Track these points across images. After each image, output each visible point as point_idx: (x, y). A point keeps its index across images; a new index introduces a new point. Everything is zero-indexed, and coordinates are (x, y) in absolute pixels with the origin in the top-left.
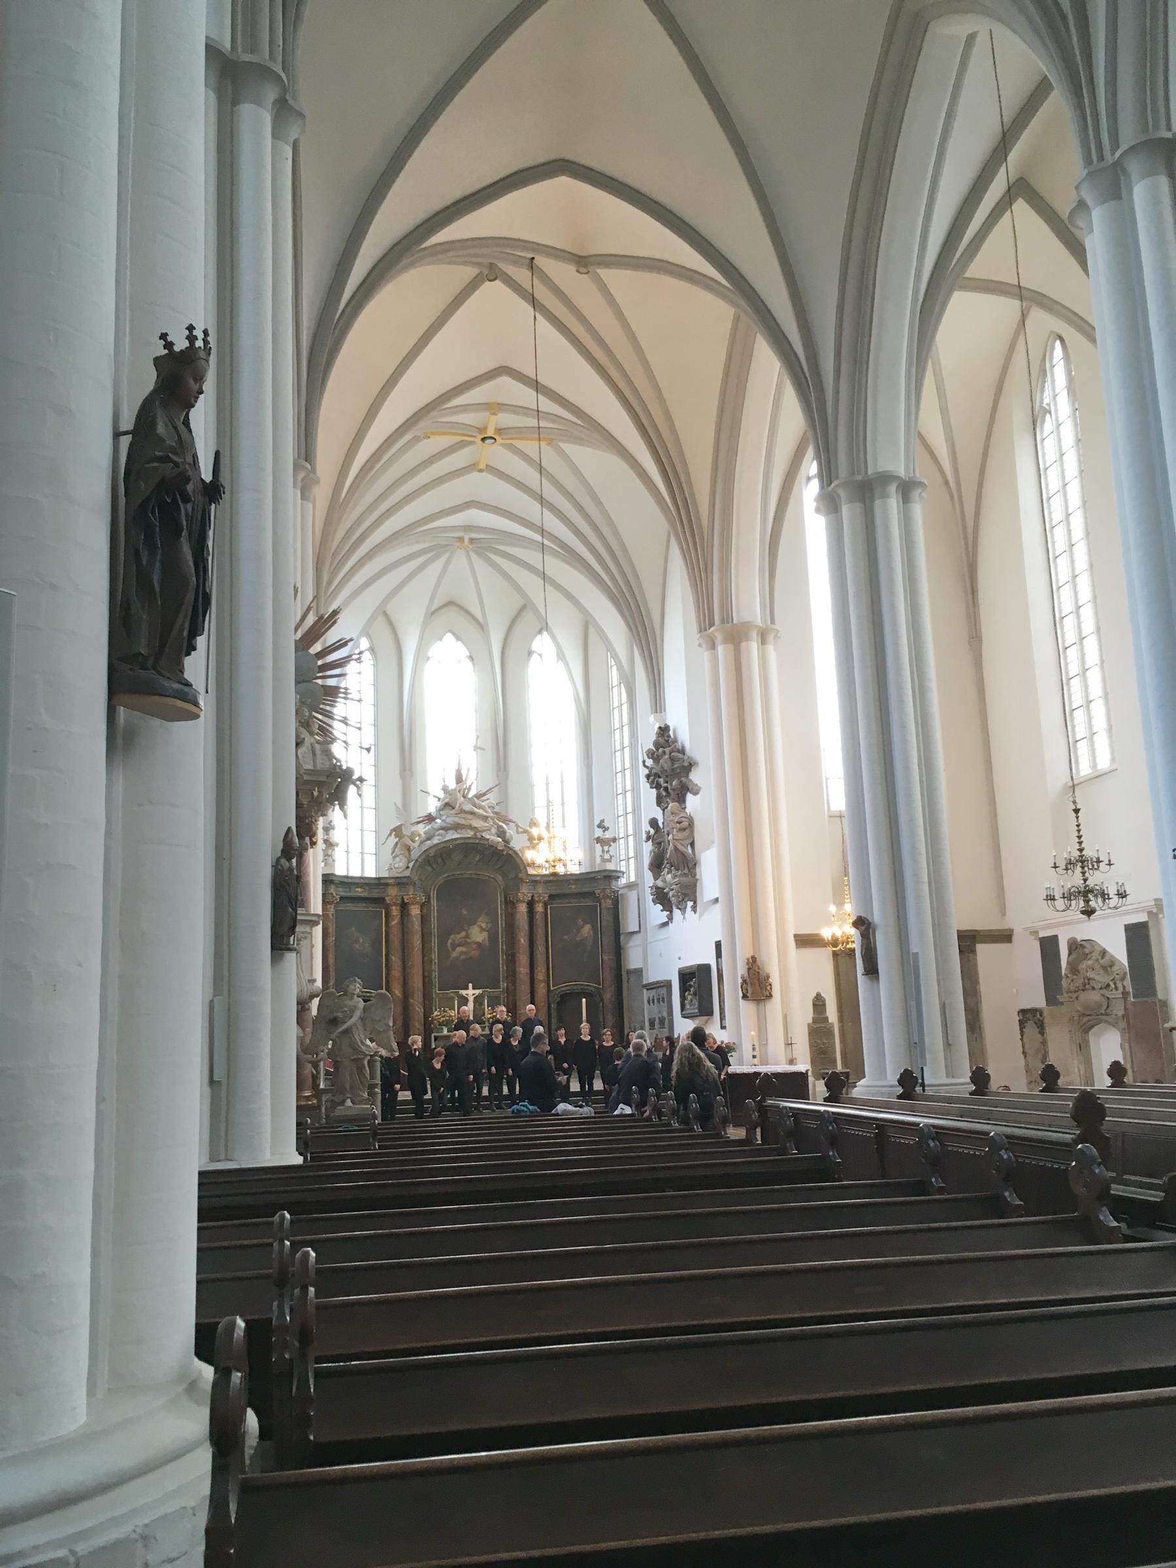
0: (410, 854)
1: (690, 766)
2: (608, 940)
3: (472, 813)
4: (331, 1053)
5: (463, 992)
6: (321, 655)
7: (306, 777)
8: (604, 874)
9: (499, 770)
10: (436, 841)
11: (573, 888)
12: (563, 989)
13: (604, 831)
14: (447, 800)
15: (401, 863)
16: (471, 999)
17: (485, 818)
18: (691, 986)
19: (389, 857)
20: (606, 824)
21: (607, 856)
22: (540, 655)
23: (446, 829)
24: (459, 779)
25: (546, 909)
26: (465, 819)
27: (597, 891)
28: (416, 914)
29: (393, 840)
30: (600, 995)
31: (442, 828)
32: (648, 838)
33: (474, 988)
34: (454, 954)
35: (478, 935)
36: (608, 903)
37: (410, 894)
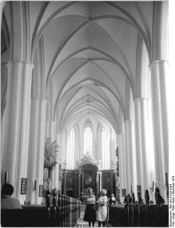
2: (112, 182)
6: (54, 146)
7: (50, 163)
15: (77, 167)
19: (75, 167)
24: (87, 153)
29: (76, 163)
30: (111, 191)
31: (84, 161)
34: (86, 183)
35: (90, 180)
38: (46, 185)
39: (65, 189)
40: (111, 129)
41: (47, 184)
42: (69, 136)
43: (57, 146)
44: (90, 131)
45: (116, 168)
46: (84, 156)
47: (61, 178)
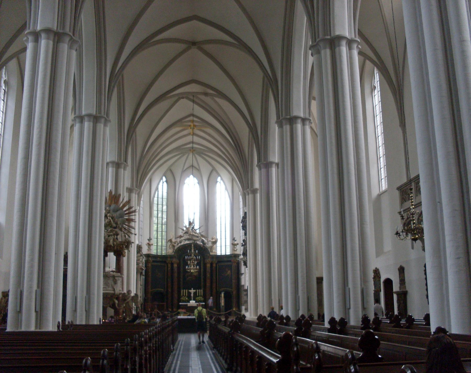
0: (174, 248)
3: (193, 235)
4: (124, 307)
5: (190, 291)
6: (125, 211)
7: (118, 243)
9: (206, 220)
10: (182, 244)
11: (225, 259)
14: (186, 231)
17: (198, 237)
20: (235, 239)
21: (235, 249)
22: (220, 183)
23: (185, 240)
24: (190, 224)
27: (232, 260)
28: (176, 267)
29: (169, 243)
30: (232, 292)
32: (242, 246)
33: (193, 289)
37: (175, 260)
38: (112, 285)
39: (150, 290)
40: (233, 180)
41: (113, 283)
42: (157, 192)
43: (133, 209)
44: (194, 184)
45: (242, 253)
46: (185, 229)
47: (141, 271)
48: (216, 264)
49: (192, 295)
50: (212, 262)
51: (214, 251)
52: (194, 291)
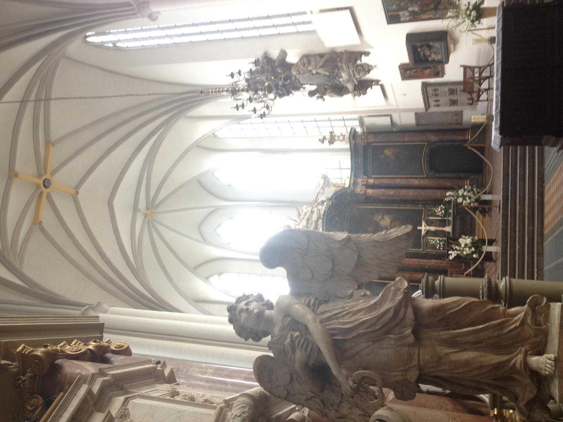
1: (267, 58)
5: (423, 232)
8: (351, 139)
12: (426, 168)
13: (326, 139)
16: (428, 228)
17: (312, 212)
18: (424, 55)
20: (321, 138)
21: (341, 138)
25: (372, 178)
26: (311, 224)
33: (421, 226)
36: (371, 139)
48: (369, 178)
49: (433, 228)
50: (363, 185)
51: (343, 182)
52: (423, 224)
